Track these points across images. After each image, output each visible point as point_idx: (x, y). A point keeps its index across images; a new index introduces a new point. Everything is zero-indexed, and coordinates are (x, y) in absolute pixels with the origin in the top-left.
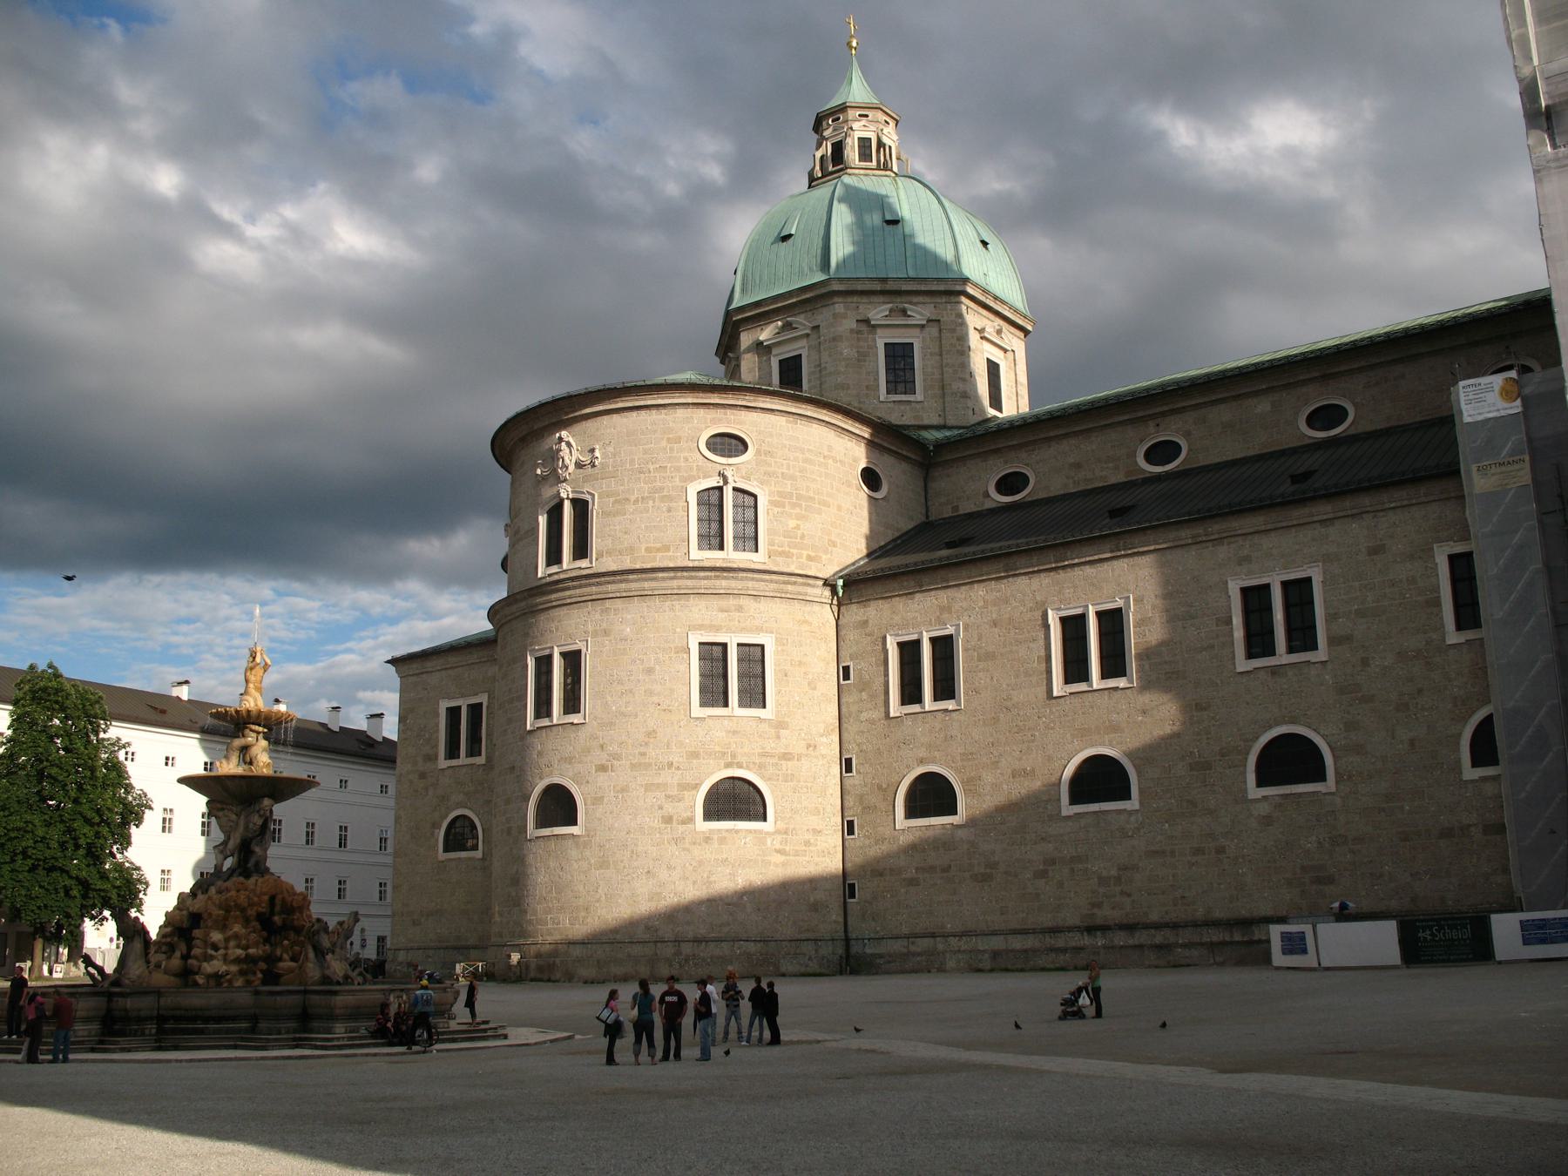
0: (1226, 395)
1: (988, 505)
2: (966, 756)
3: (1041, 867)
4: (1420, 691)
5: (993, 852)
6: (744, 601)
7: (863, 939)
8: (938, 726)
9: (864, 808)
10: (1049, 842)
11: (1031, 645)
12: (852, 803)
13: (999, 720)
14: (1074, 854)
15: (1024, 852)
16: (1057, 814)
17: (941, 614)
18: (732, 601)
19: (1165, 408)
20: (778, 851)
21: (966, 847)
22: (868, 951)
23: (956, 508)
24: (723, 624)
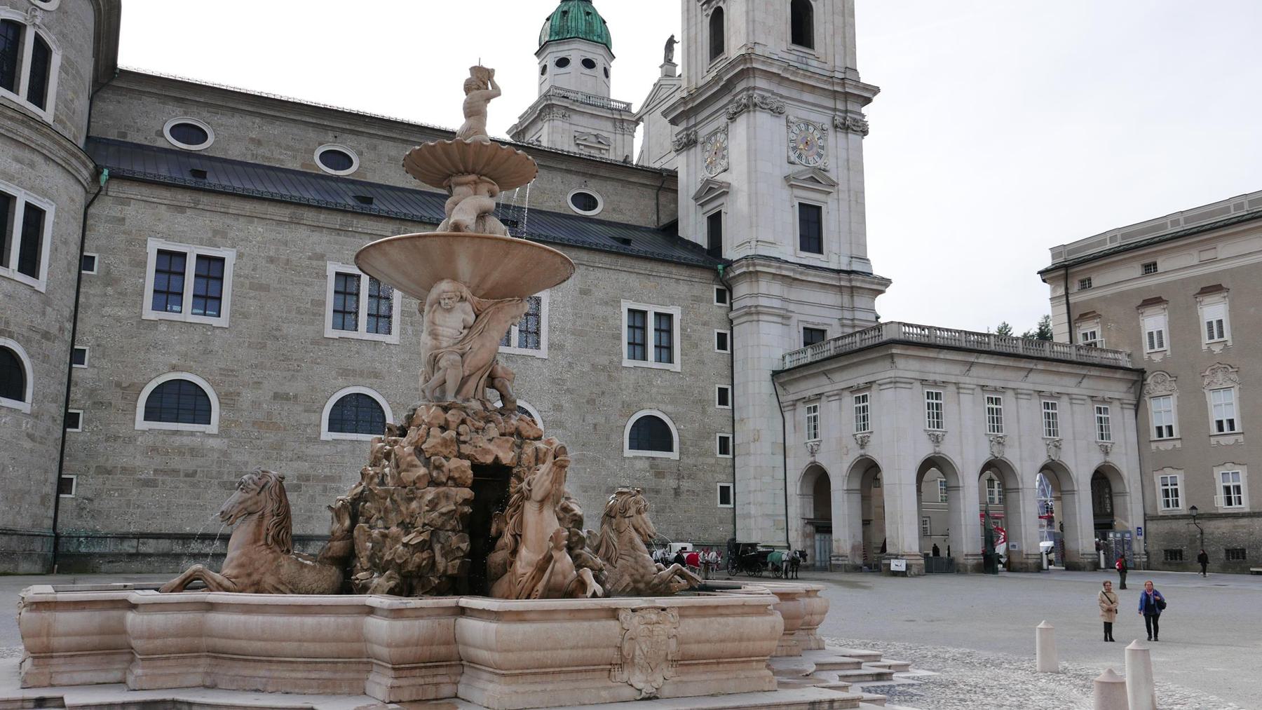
0: (398, 137)
1: (160, 143)
2: (227, 372)
3: (295, 482)
4: (603, 393)
5: (247, 462)
6: (38, 159)
7: (80, 537)
8: (197, 338)
9: (94, 403)
10: (306, 461)
11: (308, 289)
12: (79, 396)
13: (265, 346)
14: (329, 474)
15: (278, 466)
16: (316, 438)
17: (214, 236)
18: (27, 155)
19: (348, 127)
20: (30, 437)
21: (216, 455)
22: (83, 550)
23: (124, 135)
24: (16, 176)
